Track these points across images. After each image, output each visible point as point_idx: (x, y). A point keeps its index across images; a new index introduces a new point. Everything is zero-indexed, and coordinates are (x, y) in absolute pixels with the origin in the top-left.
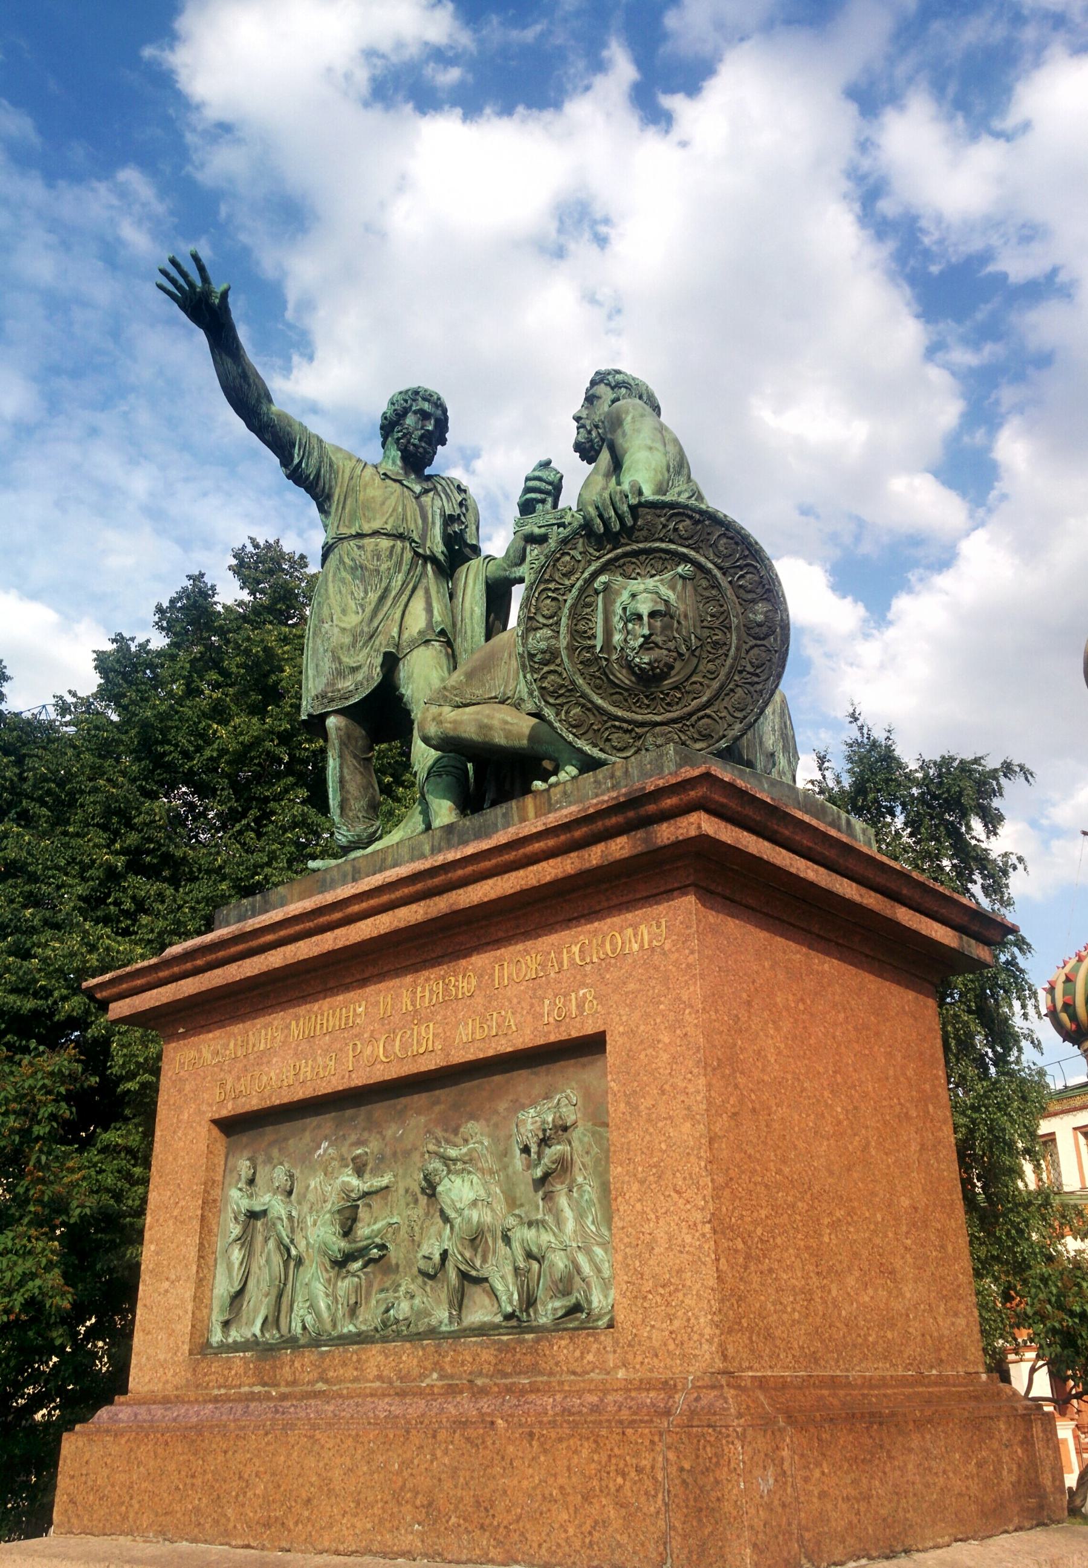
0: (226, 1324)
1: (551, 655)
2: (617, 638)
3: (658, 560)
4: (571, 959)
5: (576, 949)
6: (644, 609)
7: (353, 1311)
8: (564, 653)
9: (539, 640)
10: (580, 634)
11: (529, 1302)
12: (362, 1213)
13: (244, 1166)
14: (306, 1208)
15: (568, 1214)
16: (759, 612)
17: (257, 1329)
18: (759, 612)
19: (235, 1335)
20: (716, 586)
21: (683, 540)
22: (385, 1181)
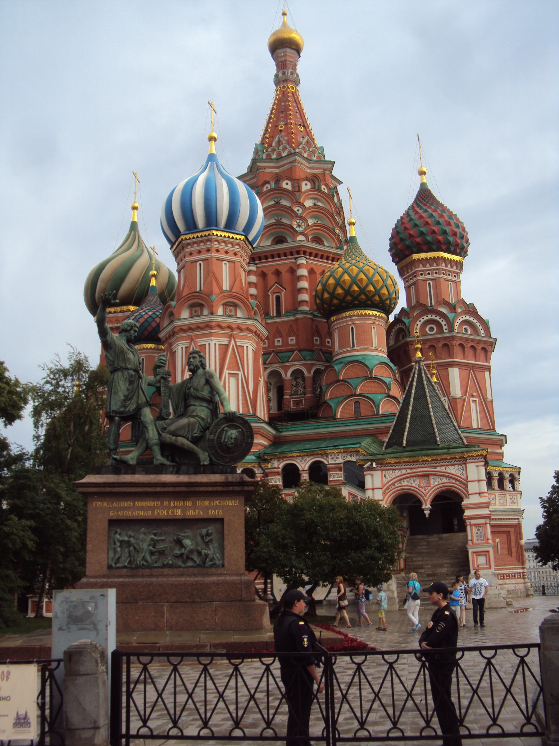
0: (116, 563)
1: (213, 440)
2: (226, 440)
3: (236, 427)
4: (216, 504)
5: (218, 502)
6: (233, 437)
7: (156, 562)
8: (215, 442)
9: (212, 437)
10: (219, 437)
11: (204, 563)
12: (157, 544)
13: (119, 530)
14: (138, 541)
15: (212, 548)
16: (250, 441)
17: (126, 564)
18: (250, 441)
19: (118, 565)
20: (244, 434)
21: (240, 424)
22: (163, 538)
